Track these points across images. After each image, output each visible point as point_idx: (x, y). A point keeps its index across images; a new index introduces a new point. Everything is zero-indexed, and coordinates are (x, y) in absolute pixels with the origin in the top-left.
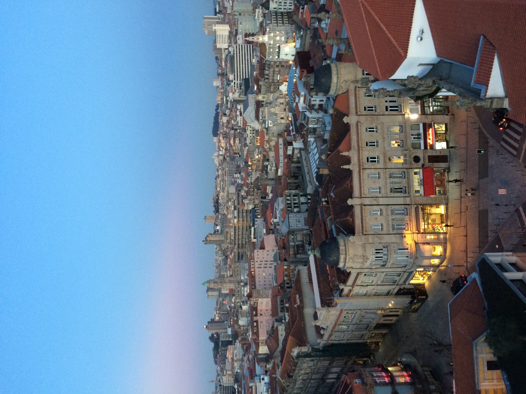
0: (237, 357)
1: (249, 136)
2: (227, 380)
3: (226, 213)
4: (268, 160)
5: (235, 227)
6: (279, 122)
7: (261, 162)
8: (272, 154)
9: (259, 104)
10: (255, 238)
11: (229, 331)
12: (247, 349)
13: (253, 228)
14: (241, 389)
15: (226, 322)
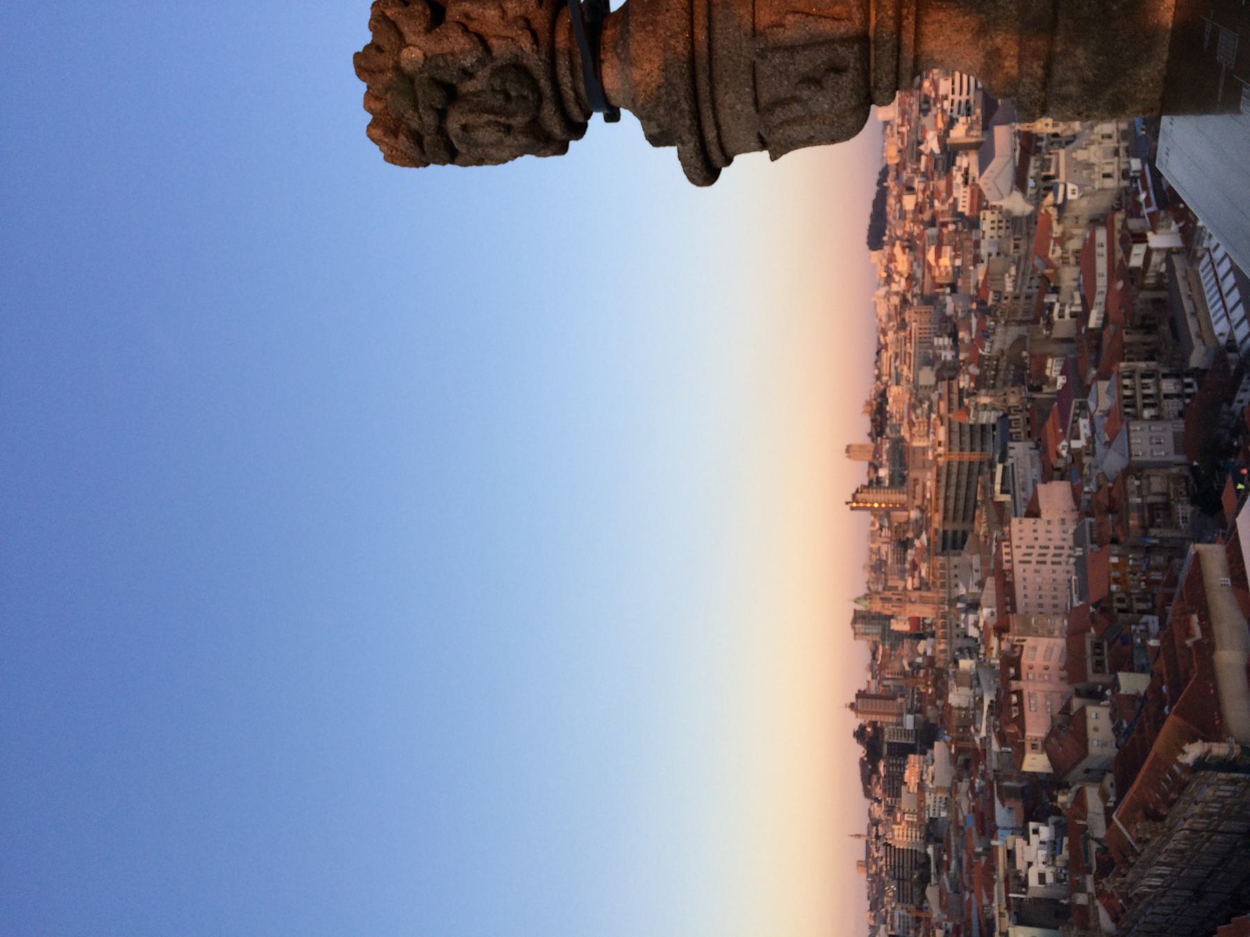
0: (936, 783)
1: (987, 236)
2: (902, 835)
3: (907, 436)
4: (1056, 290)
5: (939, 469)
6: (1097, 185)
7: (1035, 299)
8: (1069, 276)
9: (1029, 145)
10: (1003, 492)
11: (909, 722)
12: (967, 760)
13: (999, 468)
14: (949, 856)
15: (900, 700)
